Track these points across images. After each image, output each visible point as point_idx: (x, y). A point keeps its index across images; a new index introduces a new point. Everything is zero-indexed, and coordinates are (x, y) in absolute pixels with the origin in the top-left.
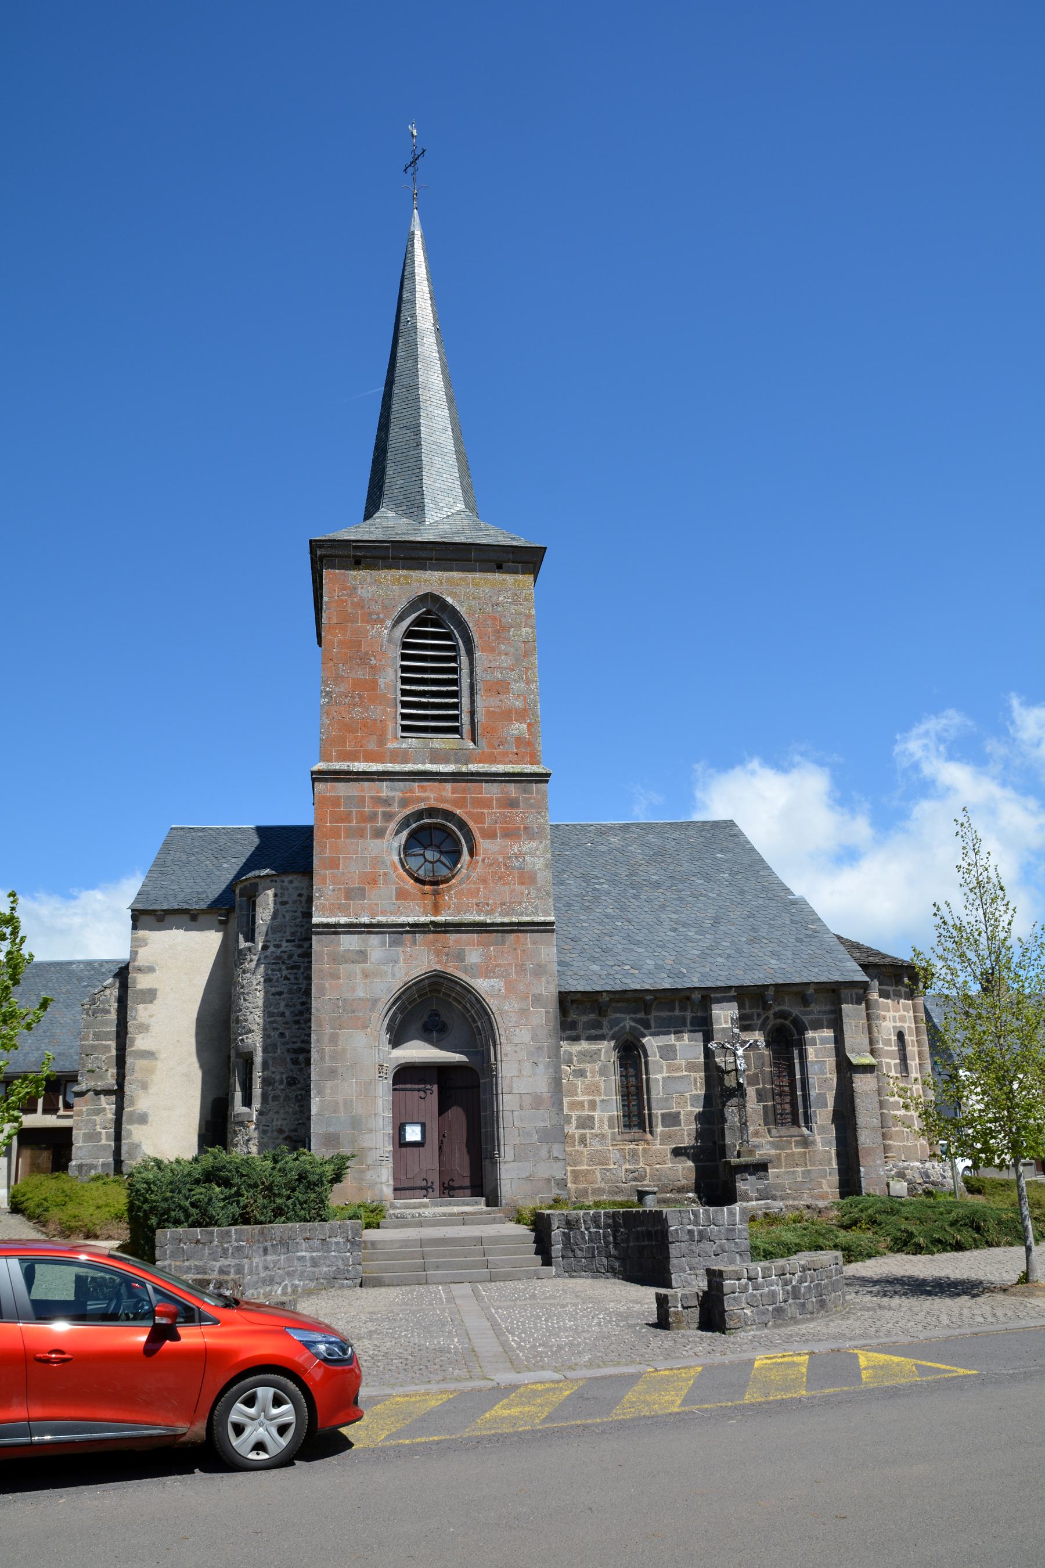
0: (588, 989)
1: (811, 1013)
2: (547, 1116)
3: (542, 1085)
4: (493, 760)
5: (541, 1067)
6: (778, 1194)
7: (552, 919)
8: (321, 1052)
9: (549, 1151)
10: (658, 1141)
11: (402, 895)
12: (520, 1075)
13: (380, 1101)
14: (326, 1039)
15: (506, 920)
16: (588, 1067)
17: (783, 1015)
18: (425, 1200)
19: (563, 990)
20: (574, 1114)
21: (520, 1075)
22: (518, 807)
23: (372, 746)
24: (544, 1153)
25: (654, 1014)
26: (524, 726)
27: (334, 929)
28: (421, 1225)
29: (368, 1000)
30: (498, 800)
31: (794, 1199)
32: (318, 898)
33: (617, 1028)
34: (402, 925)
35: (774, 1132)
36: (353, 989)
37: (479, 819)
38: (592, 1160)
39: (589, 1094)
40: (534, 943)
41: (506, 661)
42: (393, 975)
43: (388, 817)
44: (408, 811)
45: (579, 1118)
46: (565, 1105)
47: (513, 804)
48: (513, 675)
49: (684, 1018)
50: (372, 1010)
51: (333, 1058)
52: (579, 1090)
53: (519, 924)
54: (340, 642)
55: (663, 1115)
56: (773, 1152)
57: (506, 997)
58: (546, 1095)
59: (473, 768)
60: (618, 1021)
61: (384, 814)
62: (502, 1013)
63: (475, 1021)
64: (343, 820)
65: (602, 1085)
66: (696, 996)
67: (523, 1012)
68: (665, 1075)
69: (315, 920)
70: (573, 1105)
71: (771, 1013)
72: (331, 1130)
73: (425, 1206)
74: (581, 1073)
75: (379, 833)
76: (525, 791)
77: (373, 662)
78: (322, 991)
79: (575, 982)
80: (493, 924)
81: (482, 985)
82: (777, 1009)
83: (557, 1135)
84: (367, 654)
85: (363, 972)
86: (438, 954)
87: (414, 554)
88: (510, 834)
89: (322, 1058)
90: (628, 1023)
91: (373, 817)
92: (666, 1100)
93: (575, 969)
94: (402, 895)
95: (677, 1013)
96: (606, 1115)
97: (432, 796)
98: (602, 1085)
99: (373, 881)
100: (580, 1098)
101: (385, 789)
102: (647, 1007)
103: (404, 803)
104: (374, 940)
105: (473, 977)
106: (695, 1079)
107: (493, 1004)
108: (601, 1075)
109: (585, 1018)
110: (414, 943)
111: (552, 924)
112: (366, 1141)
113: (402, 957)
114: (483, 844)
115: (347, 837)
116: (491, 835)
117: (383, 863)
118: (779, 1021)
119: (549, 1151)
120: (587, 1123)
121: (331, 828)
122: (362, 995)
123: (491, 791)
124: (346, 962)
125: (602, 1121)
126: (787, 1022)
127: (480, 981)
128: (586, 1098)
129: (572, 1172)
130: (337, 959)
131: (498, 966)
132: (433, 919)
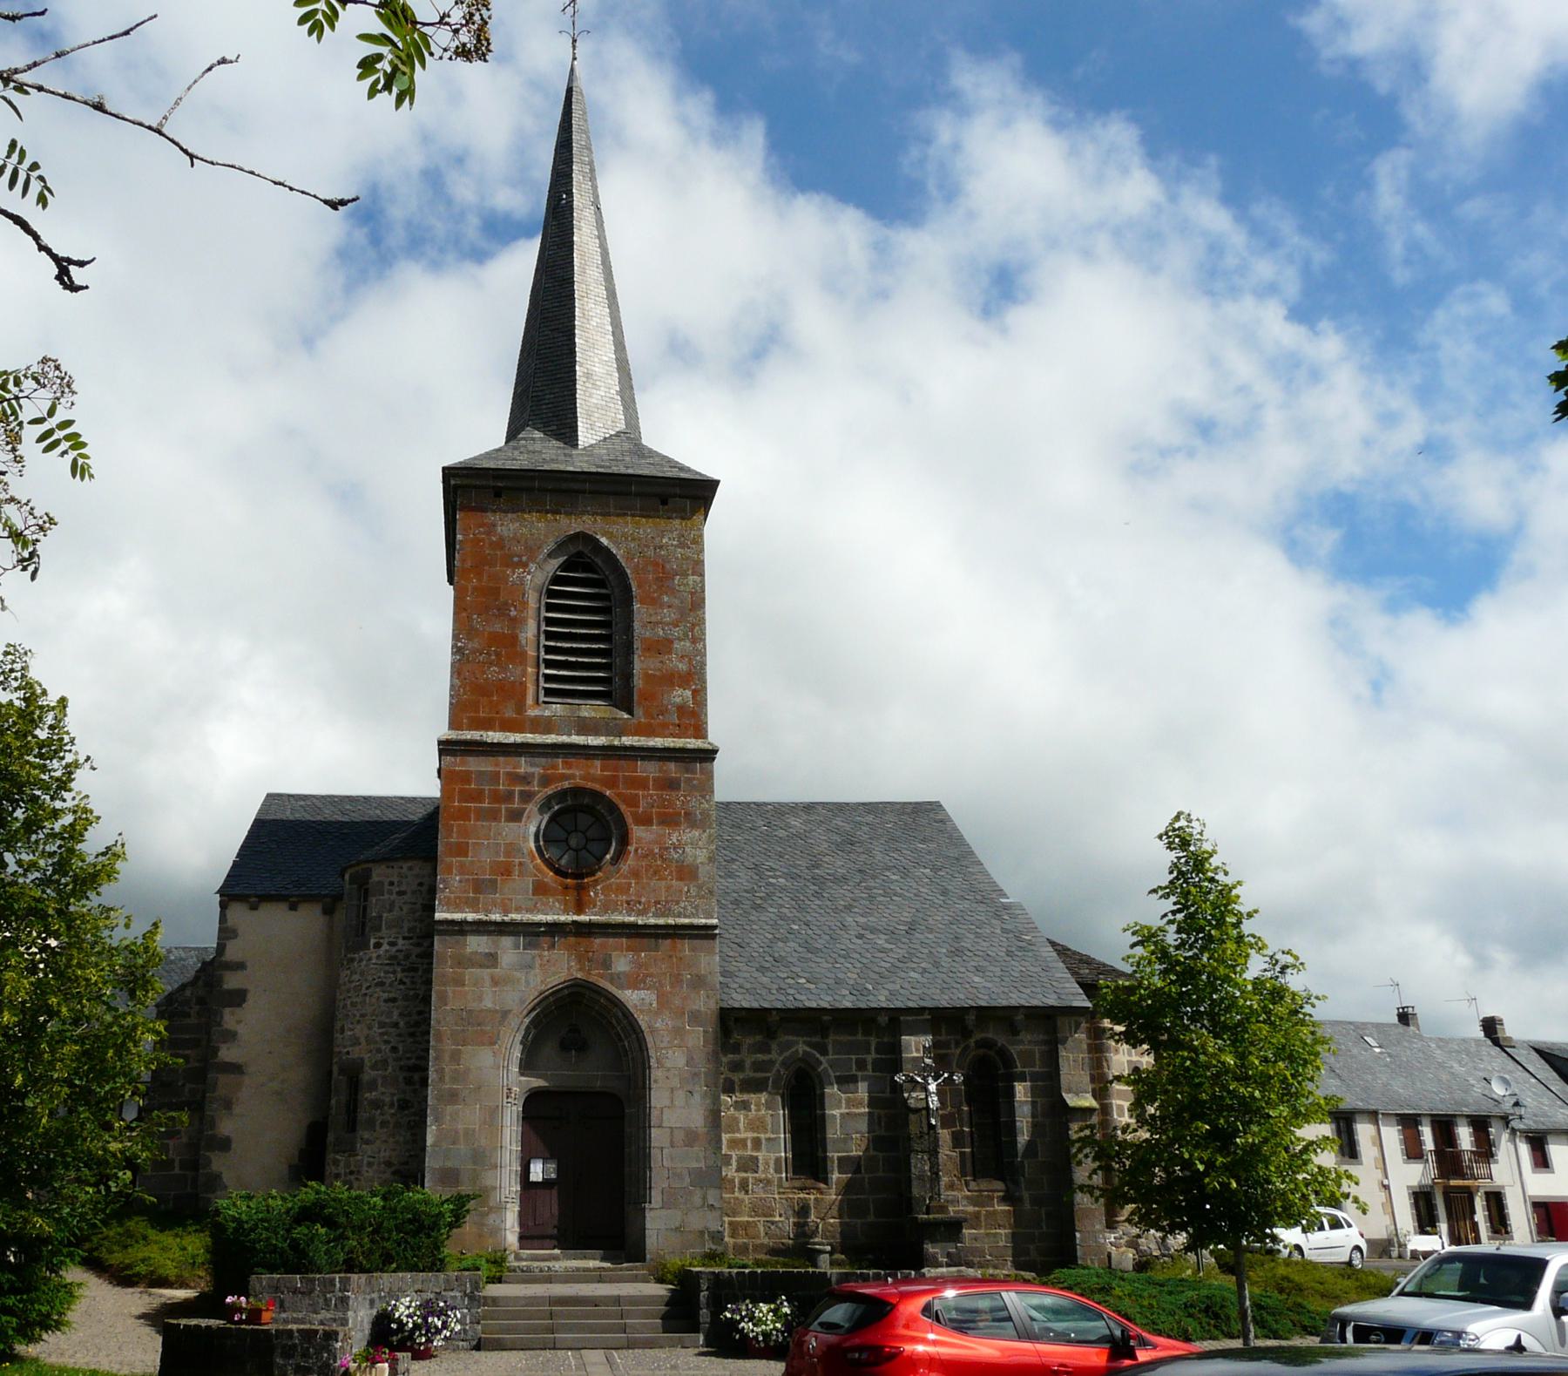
0: (755, 1005)
1: (1021, 1042)
2: (702, 1154)
3: (696, 1118)
4: (649, 732)
5: (697, 1097)
6: (976, 1260)
7: (715, 921)
8: (441, 1071)
9: (704, 1198)
10: (833, 1191)
11: (540, 889)
12: (672, 1106)
13: (507, 1132)
14: (447, 1057)
15: (661, 921)
16: (752, 1097)
17: (986, 1044)
18: (557, 1251)
19: (725, 1005)
20: (734, 1154)
21: (672, 1106)
22: (678, 789)
23: (510, 713)
24: (697, 1200)
25: (832, 1038)
26: (688, 693)
27: (461, 928)
28: (549, 1280)
29: (496, 1011)
30: (654, 780)
31: (995, 1267)
32: (443, 890)
33: (787, 1054)
34: (539, 924)
35: (973, 1185)
36: (480, 999)
37: (633, 802)
38: (754, 1211)
39: (752, 1130)
40: (693, 950)
41: (668, 615)
42: (527, 982)
43: (527, 797)
44: (549, 791)
45: (740, 1158)
46: (724, 1142)
47: (671, 785)
48: (677, 632)
49: (868, 1044)
50: (501, 1022)
51: (454, 1080)
52: (741, 1125)
53: (676, 927)
54: (475, 589)
55: (840, 1159)
56: (971, 1209)
57: (658, 1013)
59: (627, 741)
60: (789, 1045)
61: (521, 792)
62: (653, 1031)
63: (621, 1040)
64: (473, 800)
65: (769, 1119)
66: (883, 1020)
67: (678, 1032)
68: (844, 1111)
69: (438, 916)
70: (734, 1143)
71: (972, 1041)
72: (449, 1164)
73: (556, 1258)
74: (744, 1106)
75: (515, 816)
76: (687, 771)
77: (513, 613)
78: (443, 999)
79: (739, 997)
80: (646, 926)
81: (631, 998)
82: (978, 1036)
83: (711, 1178)
84: (506, 603)
85: (492, 978)
86: (580, 960)
87: (564, 486)
88: (670, 820)
89: (441, 1079)
90: (802, 1048)
91: (509, 797)
92: (845, 1141)
93: (741, 981)
94: (540, 889)
95: (860, 1037)
96: (773, 1156)
97: (576, 774)
98: (769, 1119)
99: (506, 870)
100: (743, 1136)
101: (523, 766)
102: (824, 1031)
103: (546, 781)
104: (507, 941)
105: (621, 987)
106: (879, 1117)
107: (643, 1021)
108: (768, 1108)
109: (749, 1041)
110: (552, 946)
111: (715, 927)
112: (488, 1179)
113: (538, 962)
114: (638, 832)
115: (477, 819)
116: (645, 821)
117: (520, 850)
118: (981, 1051)
119: (704, 1198)
120: (749, 1165)
121: (460, 809)
122: (490, 1005)
124: (473, 966)
125: (767, 1163)
126: (992, 1053)
127: (628, 992)
128: (750, 1135)
129: (730, 1223)
130: (463, 962)
131: (651, 975)
132: (576, 918)
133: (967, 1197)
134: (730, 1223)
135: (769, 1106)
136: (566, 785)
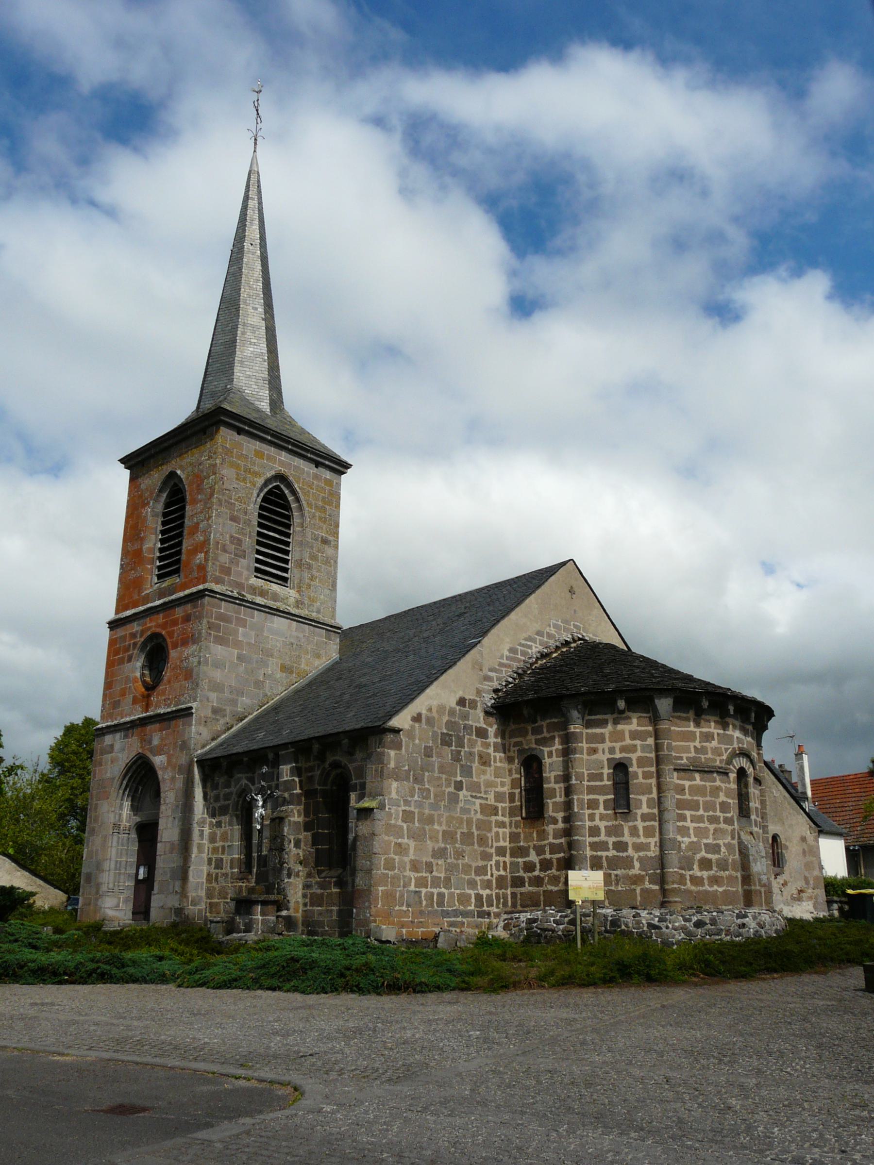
4: (184, 587)
6: (320, 930)
16: (223, 818)
23: (136, 597)
30: (182, 617)
37: (171, 634)
41: (200, 506)
47: (187, 619)
48: (202, 516)
56: (319, 891)
58: (176, 842)
60: (239, 779)
67: (173, 779)
88: (185, 643)
90: (244, 782)
96: (229, 857)
97: (152, 625)
103: (143, 632)
108: (230, 825)
123: (179, 612)
126: (334, 773)
128: (221, 844)
133: (317, 883)
134: (210, 903)
135: (231, 824)
136: (149, 633)
